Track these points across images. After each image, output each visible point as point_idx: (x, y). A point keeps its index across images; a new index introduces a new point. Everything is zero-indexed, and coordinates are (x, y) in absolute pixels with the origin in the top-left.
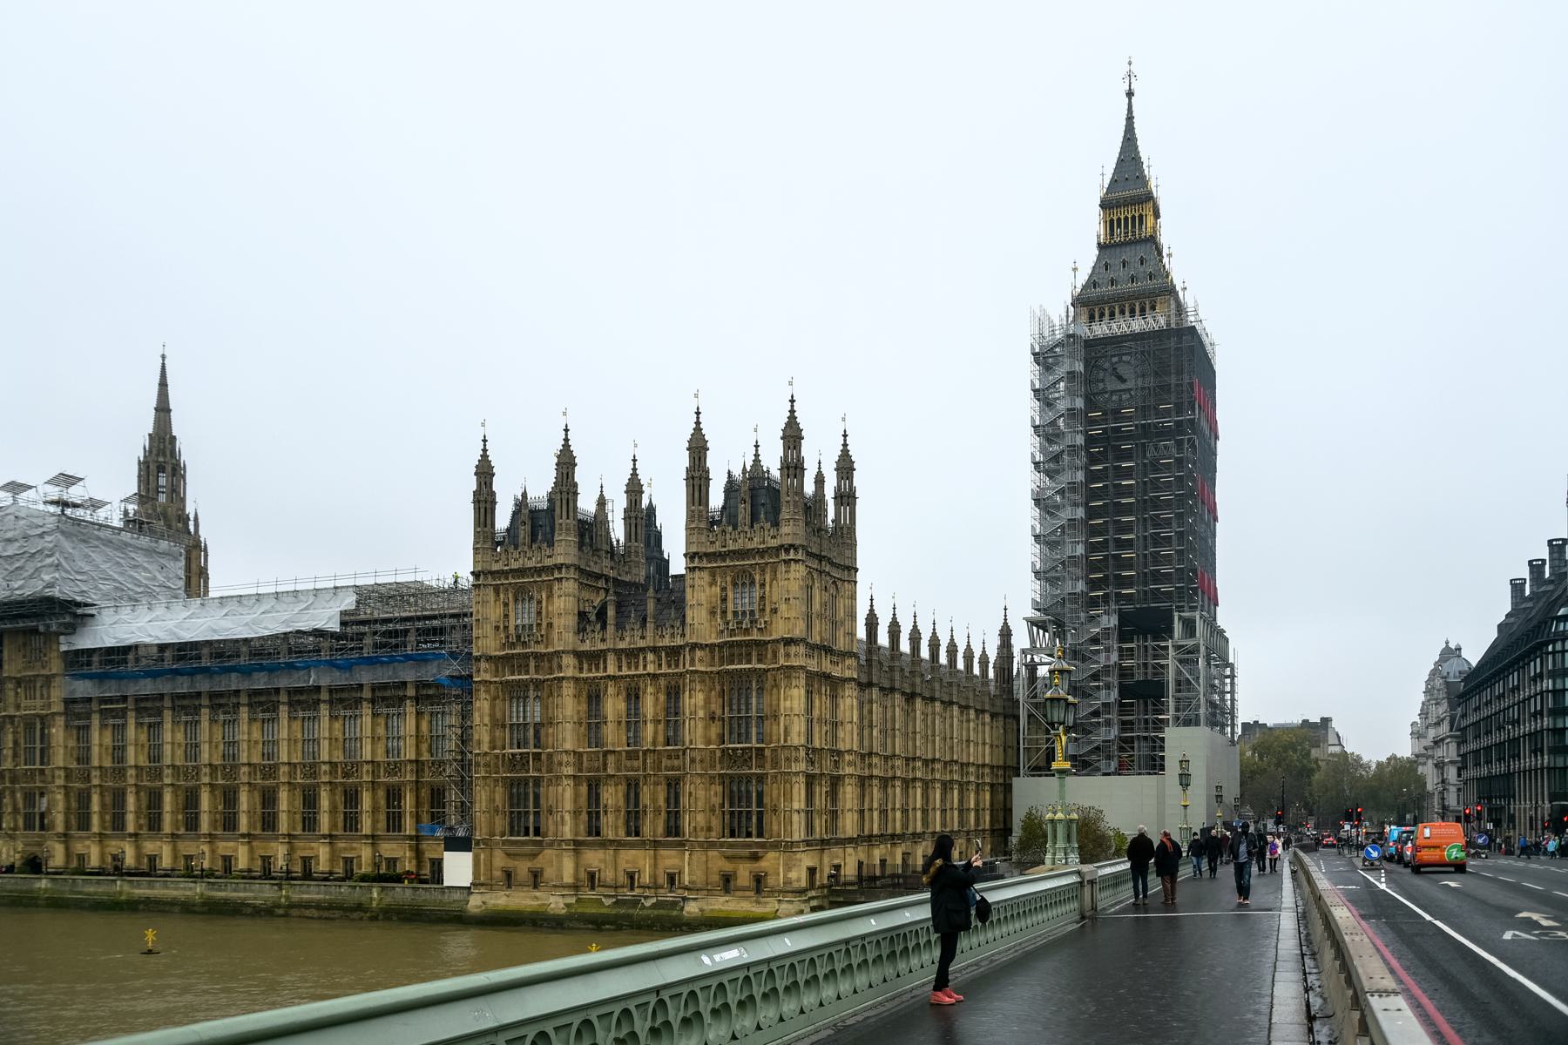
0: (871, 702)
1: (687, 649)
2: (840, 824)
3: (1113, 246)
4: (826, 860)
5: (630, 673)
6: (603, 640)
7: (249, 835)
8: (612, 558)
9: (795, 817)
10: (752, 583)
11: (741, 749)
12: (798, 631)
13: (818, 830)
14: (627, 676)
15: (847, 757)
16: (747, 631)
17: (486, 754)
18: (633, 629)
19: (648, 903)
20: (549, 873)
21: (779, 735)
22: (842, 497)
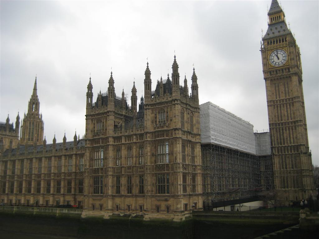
1: (145, 134)
2: (196, 189)
3: (274, 24)
4: (191, 201)
5: (129, 142)
6: (121, 133)
7: (43, 194)
8: (126, 110)
9: (179, 187)
10: (165, 112)
11: (161, 165)
12: (179, 126)
13: (188, 191)
15: (198, 167)
16: (163, 127)
17: (88, 169)
18: (130, 129)
19: (134, 215)
20: (105, 206)
21: (173, 159)
22: (193, 87)
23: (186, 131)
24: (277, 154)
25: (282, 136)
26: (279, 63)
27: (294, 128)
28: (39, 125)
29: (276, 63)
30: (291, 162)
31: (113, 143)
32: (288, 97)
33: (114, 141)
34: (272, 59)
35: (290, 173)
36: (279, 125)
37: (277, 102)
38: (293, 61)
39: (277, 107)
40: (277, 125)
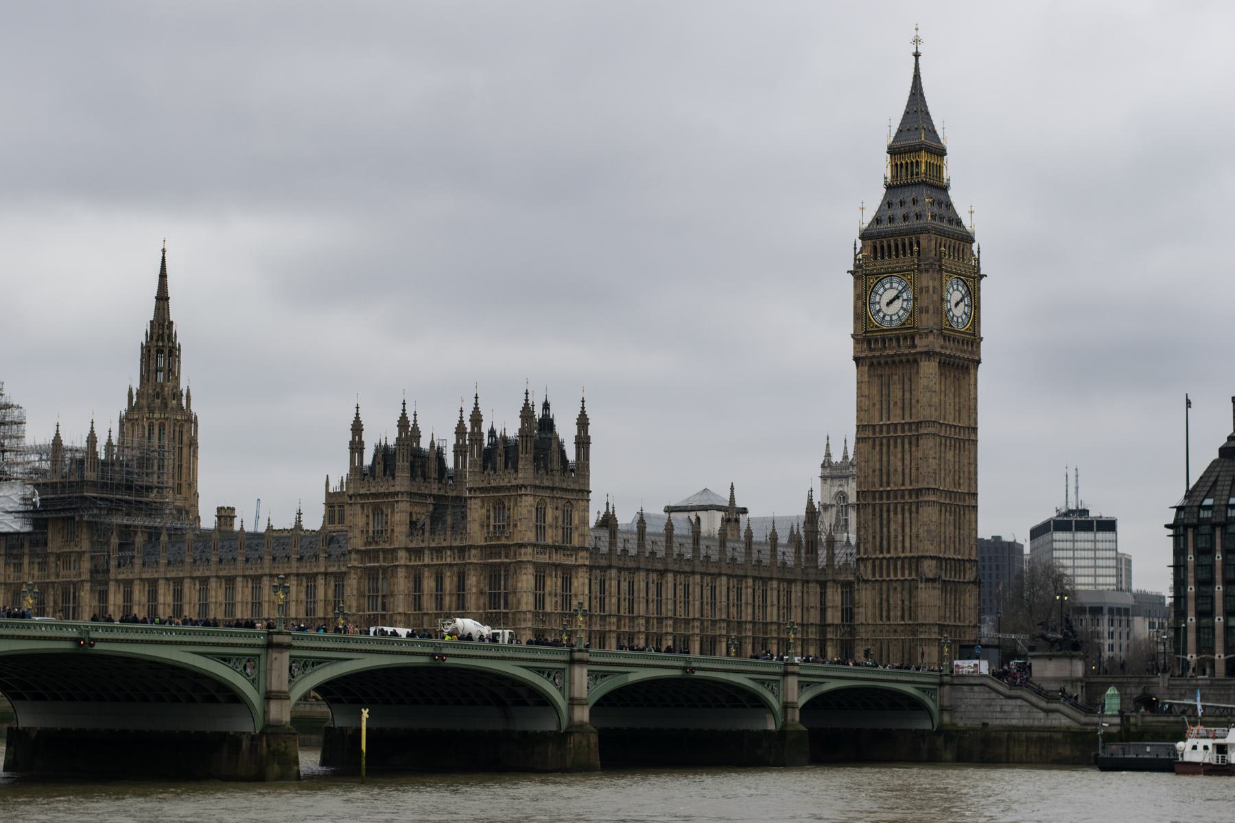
0: (610, 579)
6: (423, 541)
8: (440, 481)
10: (504, 508)
11: (496, 613)
12: (530, 537)
14: (436, 565)
16: (499, 538)
17: (354, 615)
23: (548, 546)
24: (870, 578)
25: (885, 530)
26: (891, 316)
27: (914, 508)
28: (181, 432)
29: (884, 316)
30: (900, 603)
31: (408, 561)
32: (907, 420)
33: (408, 556)
34: (875, 303)
35: (895, 631)
36: (881, 499)
37: (881, 431)
38: (924, 316)
39: (881, 445)
40: (877, 496)
